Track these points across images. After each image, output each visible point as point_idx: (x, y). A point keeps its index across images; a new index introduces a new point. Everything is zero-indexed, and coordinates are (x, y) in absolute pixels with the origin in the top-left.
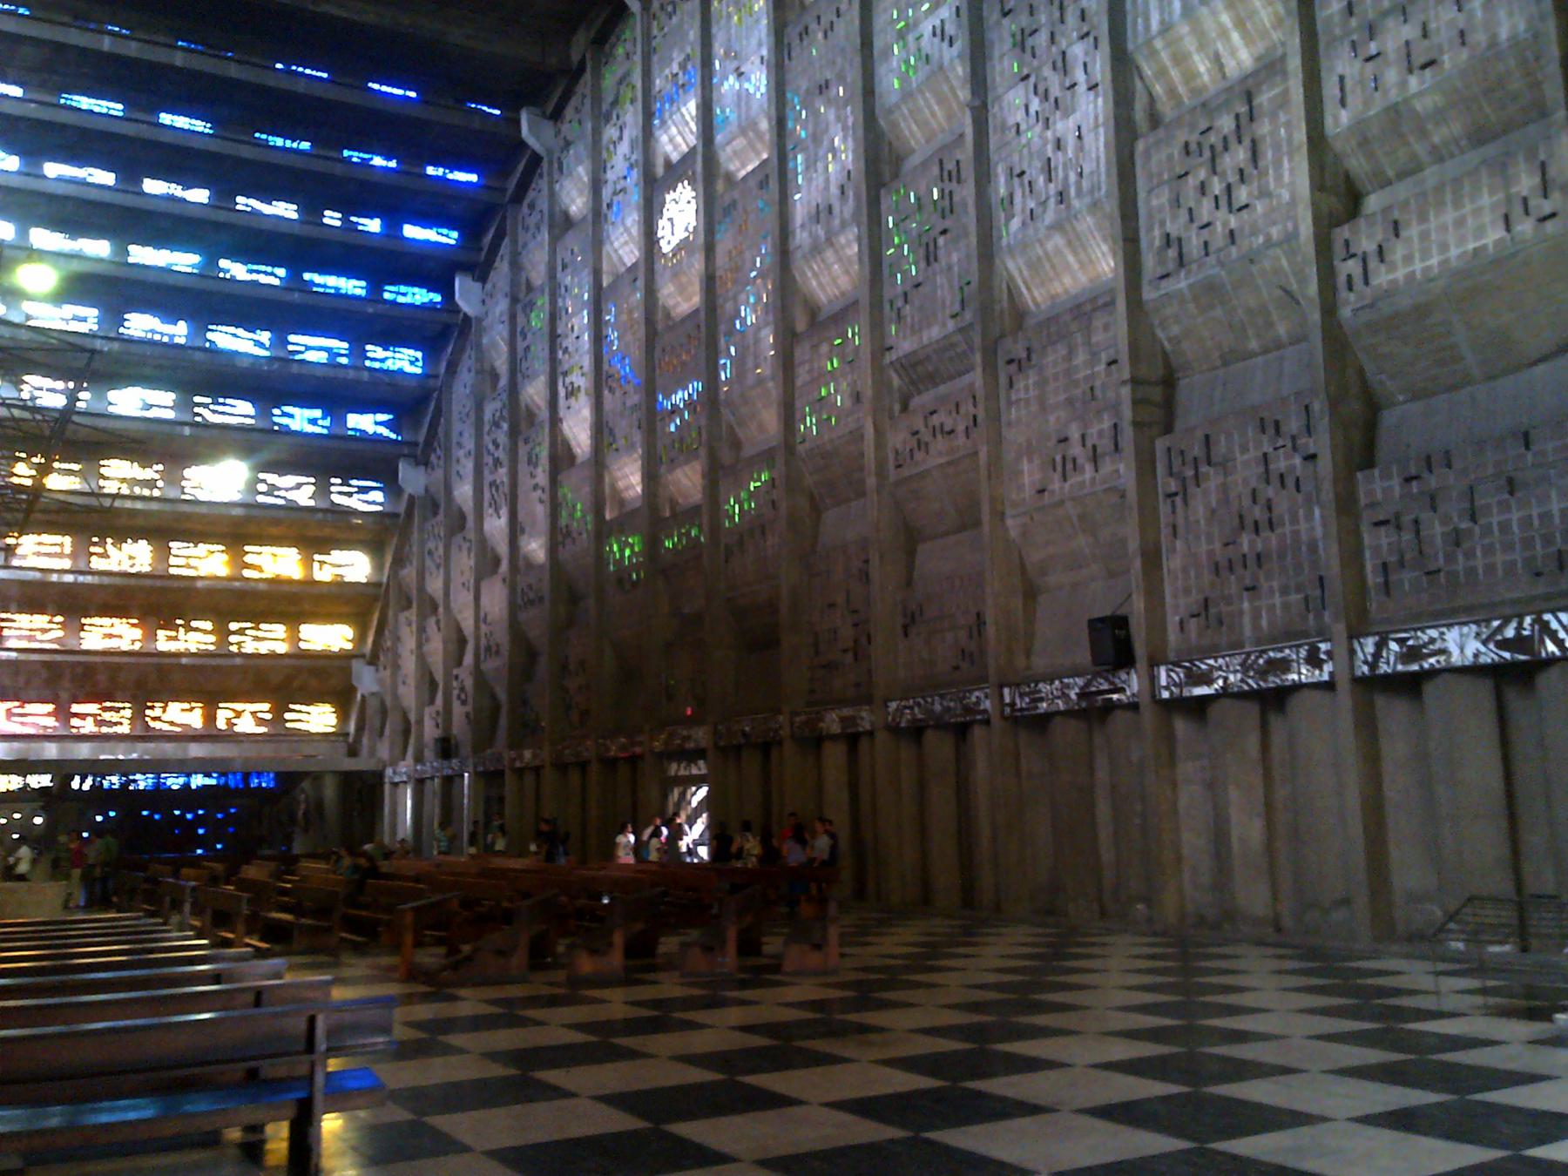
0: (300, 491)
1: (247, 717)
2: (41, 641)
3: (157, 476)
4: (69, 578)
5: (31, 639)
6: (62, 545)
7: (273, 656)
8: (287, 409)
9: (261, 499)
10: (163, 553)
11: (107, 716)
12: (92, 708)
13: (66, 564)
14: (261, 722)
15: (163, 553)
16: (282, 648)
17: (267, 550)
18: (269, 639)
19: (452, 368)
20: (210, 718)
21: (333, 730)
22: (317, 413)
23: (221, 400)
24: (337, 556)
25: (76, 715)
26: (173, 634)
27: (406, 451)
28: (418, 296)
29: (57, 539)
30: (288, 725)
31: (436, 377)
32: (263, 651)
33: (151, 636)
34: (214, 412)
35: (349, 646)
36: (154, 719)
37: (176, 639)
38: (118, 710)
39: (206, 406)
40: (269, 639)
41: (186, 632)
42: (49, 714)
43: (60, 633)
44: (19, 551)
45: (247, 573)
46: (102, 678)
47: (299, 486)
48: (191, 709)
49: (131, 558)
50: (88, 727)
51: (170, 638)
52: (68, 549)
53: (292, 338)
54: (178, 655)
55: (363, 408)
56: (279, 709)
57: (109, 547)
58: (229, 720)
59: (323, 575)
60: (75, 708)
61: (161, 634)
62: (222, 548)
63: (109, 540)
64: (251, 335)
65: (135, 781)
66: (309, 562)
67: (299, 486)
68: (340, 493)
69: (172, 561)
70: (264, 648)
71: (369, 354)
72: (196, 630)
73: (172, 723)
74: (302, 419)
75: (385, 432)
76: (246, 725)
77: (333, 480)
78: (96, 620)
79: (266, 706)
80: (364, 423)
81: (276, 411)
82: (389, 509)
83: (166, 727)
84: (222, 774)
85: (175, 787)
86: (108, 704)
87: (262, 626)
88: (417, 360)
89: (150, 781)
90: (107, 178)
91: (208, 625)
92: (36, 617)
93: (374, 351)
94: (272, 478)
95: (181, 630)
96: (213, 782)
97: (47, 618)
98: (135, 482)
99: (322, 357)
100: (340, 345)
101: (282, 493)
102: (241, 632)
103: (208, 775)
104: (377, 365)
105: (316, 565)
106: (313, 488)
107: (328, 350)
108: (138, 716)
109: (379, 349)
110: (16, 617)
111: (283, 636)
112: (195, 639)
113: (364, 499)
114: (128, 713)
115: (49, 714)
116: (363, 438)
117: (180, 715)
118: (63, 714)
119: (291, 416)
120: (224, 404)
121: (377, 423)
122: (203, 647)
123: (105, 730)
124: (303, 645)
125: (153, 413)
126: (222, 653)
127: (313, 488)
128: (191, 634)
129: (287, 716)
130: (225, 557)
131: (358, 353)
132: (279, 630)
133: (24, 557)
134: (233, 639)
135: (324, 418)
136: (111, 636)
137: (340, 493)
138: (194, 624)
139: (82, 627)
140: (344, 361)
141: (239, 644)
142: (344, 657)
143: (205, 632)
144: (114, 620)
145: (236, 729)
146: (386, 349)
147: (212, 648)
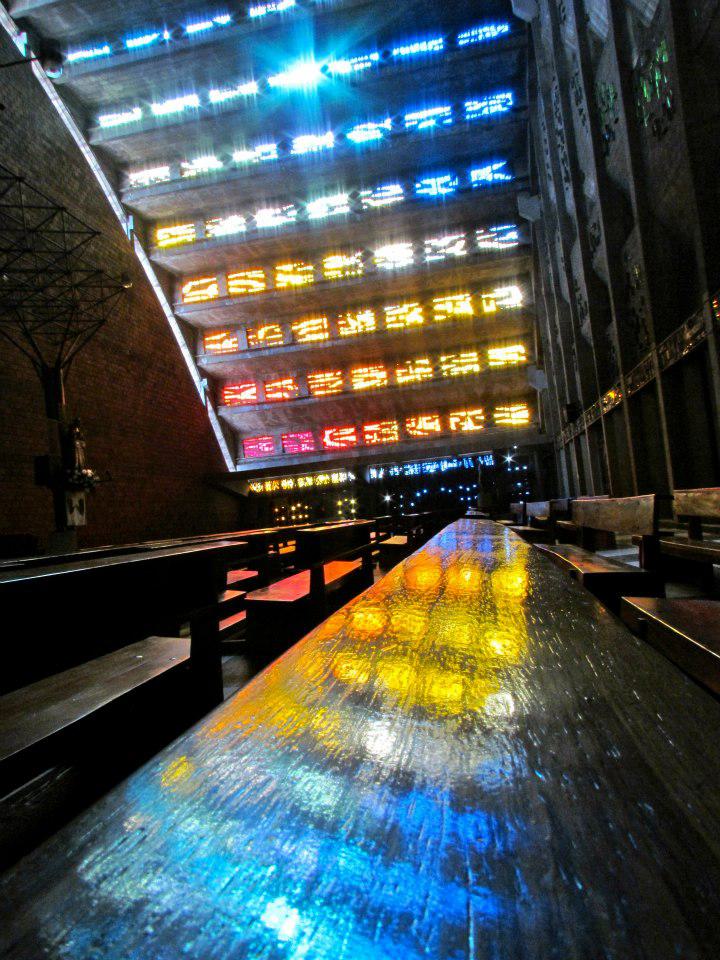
0: (450, 245)
1: (468, 421)
2: (332, 389)
3: (359, 261)
4: (328, 344)
5: (326, 388)
6: (322, 324)
7: (471, 376)
8: (426, 182)
9: (429, 259)
10: (380, 317)
11: (384, 431)
12: (374, 427)
13: (327, 335)
14: (477, 423)
15: (380, 317)
16: (477, 368)
17: (449, 298)
18: (466, 364)
19: (533, 97)
20: (445, 424)
21: (526, 421)
22: (447, 178)
23: (379, 189)
24: (499, 292)
25: (367, 433)
26: (405, 371)
27: (520, 186)
28: (491, 31)
29: (319, 321)
30: (497, 422)
31: (525, 108)
32: (465, 372)
33: (391, 375)
34: (375, 199)
35: (524, 359)
36: (412, 429)
37: (408, 374)
38: (390, 426)
39: (368, 197)
40: (466, 364)
41: (413, 369)
42: (352, 434)
43: (340, 382)
44: (300, 333)
45: (438, 318)
46: (372, 406)
47: (452, 244)
48: (433, 420)
49: (363, 324)
50: (375, 439)
51: (404, 374)
52: (326, 326)
53: (408, 117)
54: (410, 384)
55: (482, 160)
56: (489, 412)
57: (350, 320)
58: (457, 424)
59: (489, 308)
60: (368, 428)
61: (399, 372)
62: (417, 304)
63: (349, 315)
64: (377, 126)
65: (408, 470)
66: (477, 303)
67: (452, 244)
68: (484, 240)
69: (388, 320)
70: (465, 370)
71: (469, 110)
72: (420, 366)
73: (423, 431)
74: (437, 186)
75: (501, 177)
76: (469, 426)
77: (478, 232)
78: (360, 370)
79: (479, 411)
80: (485, 174)
81: (418, 185)
82: (524, 241)
83: (419, 433)
84: (460, 459)
85: (432, 471)
86: (384, 423)
87: (462, 355)
88: (508, 100)
89: (416, 468)
90: (224, 19)
91: (426, 361)
92: (327, 375)
93: (472, 106)
94: (434, 242)
95: (410, 368)
96: (455, 465)
97: (332, 374)
98: (344, 270)
99: (432, 123)
100: (446, 110)
101: (443, 251)
102: (449, 362)
103: (450, 461)
104: (474, 116)
105: (484, 301)
106: (464, 242)
107: (434, 117)
108: (402, 426)
109: (475, 103)
110: (316, 376)
111: (476, 360)
112: (419, 371)
113: (503, 239)
114: (396, 427)
115: (352, 434)
116: (485, 187)
117: (426, 425)
118: (360, 433)
119: (429, 186)
120: (381, 191)
121: (494, 172)
122: (425, 376)
123: (384, 440)
124: (491, 364)
125: (337, 211)
126: (438, 378)
127: (463, 243)
128: (418, 370)
129: (496, 416)
130: (420, 310)
131: (458, 110)
132: (473, 356)
133: (303, 336)
134: (444, 367)
135: (453, 179)
136: (369, 379)
137: (481, 240)
138: (417, 362)
139: (352, 376)
140: (449, 121)
141: (448, 371)
142: (522, 369)
143: (425, 366)
144: (371, 368)
145: (463, 429)
146: (481, 101)
147: (431, 376)
